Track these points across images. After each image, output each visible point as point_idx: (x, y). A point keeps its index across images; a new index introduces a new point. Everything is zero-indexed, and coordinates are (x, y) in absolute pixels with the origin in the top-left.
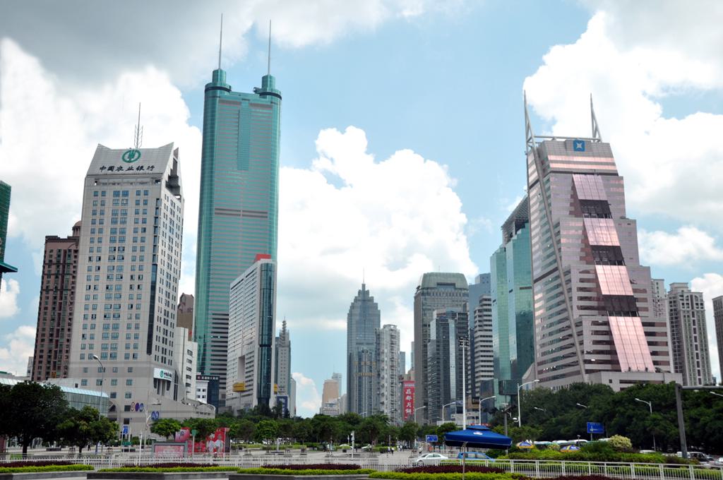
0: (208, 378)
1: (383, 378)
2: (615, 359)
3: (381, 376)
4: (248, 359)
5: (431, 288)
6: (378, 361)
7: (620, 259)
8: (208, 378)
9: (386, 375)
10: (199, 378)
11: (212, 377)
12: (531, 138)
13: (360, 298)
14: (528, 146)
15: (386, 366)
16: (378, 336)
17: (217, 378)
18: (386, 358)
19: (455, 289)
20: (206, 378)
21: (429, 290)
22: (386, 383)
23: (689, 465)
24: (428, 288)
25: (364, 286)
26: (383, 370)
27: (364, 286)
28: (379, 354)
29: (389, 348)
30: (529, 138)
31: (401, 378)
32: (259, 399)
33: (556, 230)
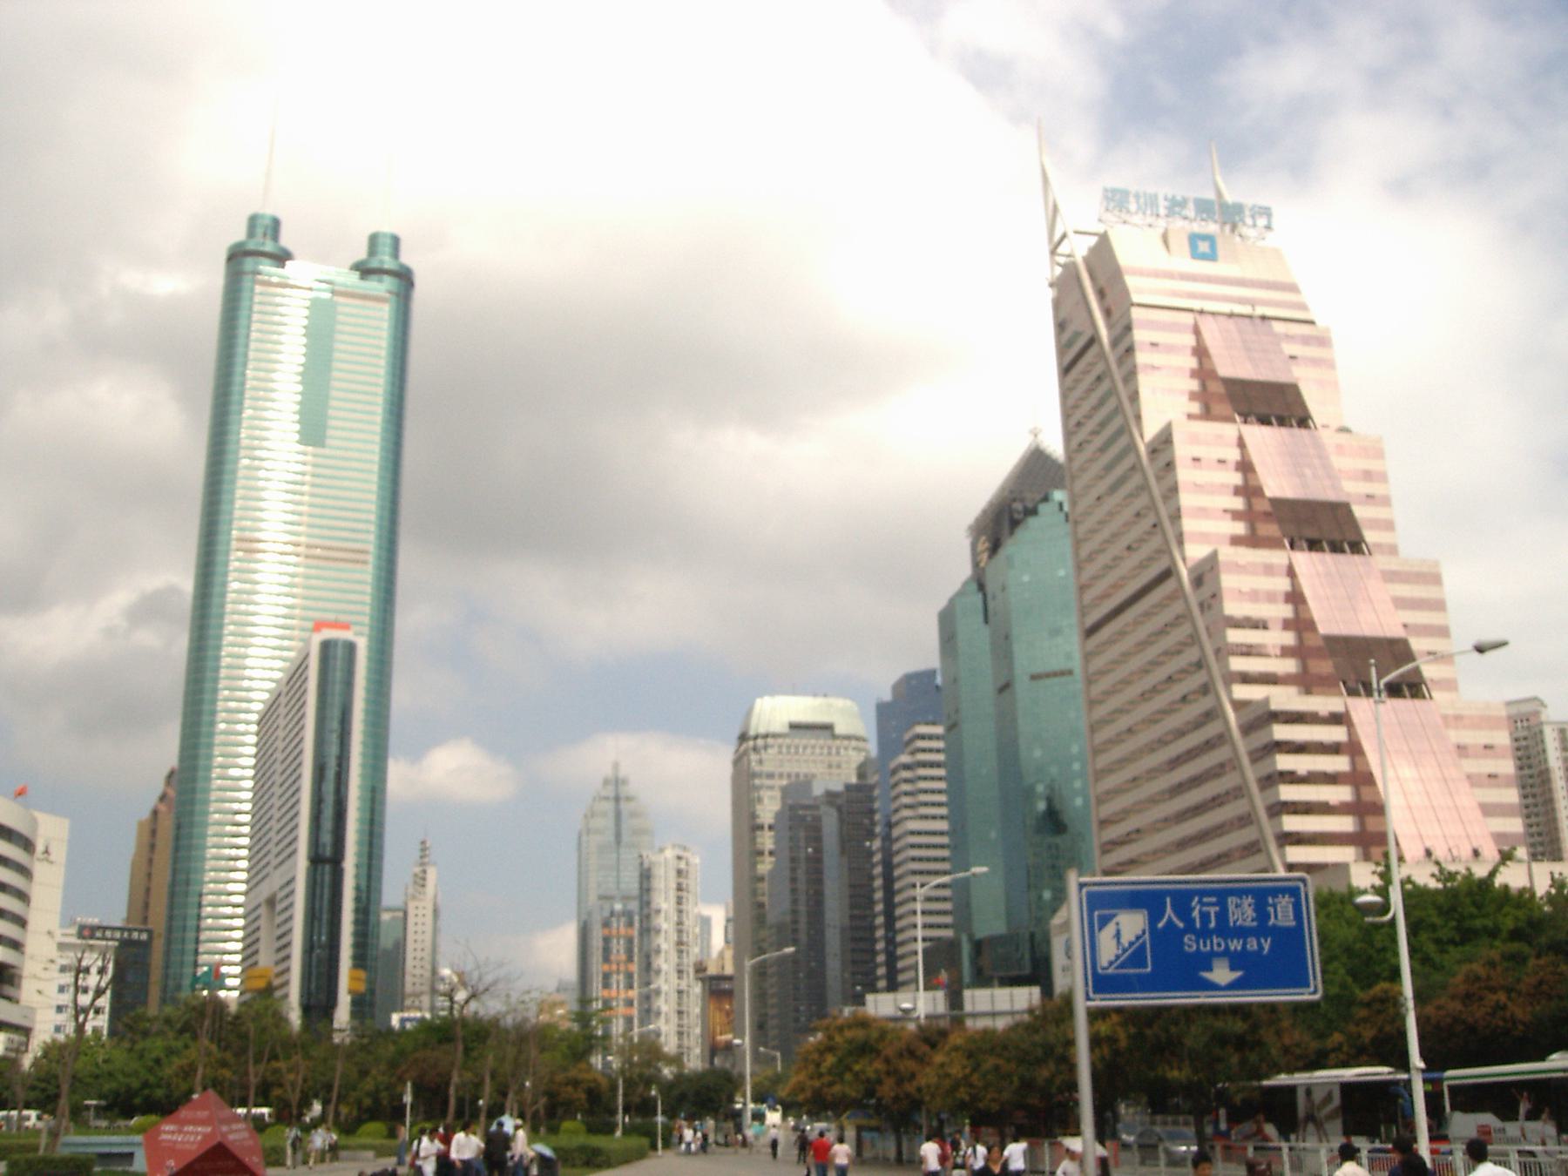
0: (118, 935)
1: (658, 972)
2: (1381, 829)
3: (655, 966)
4: (282, 900)
5: (775, 736)
6: (647, 930)
7: (1353, 538)
8: (118, 935)
9: (665, 963)
10: (86, 933)
11: (130, 930)
12: (1064, 236)
13: (604, 793)
14: (1054, 263)
15: (665, 943)
16: (646, 876)
17: (144, 937)
18: (665, 923)
19: (834, 737)
20: (108, 934)
21: (770, 741)
22: (666, 983)
23: (1453, 1146)
24: (766, 736)
25: (616, 766)
26: (658, 951)
27: (616, 766)
28: (648, 917)
29: (673, 900)
30: (1057, 237)
31: (700, 968)
32: (307, 1009)
33: (1161, 462)
